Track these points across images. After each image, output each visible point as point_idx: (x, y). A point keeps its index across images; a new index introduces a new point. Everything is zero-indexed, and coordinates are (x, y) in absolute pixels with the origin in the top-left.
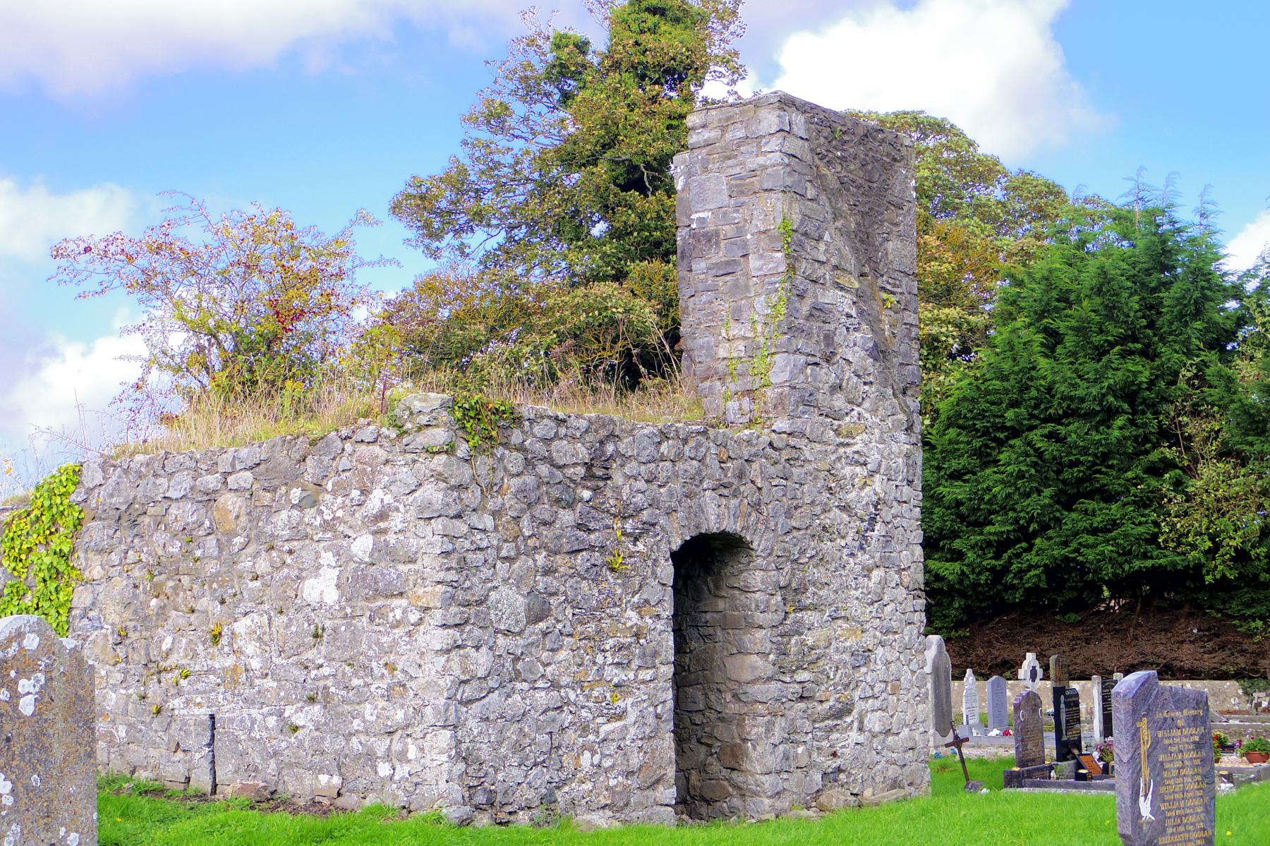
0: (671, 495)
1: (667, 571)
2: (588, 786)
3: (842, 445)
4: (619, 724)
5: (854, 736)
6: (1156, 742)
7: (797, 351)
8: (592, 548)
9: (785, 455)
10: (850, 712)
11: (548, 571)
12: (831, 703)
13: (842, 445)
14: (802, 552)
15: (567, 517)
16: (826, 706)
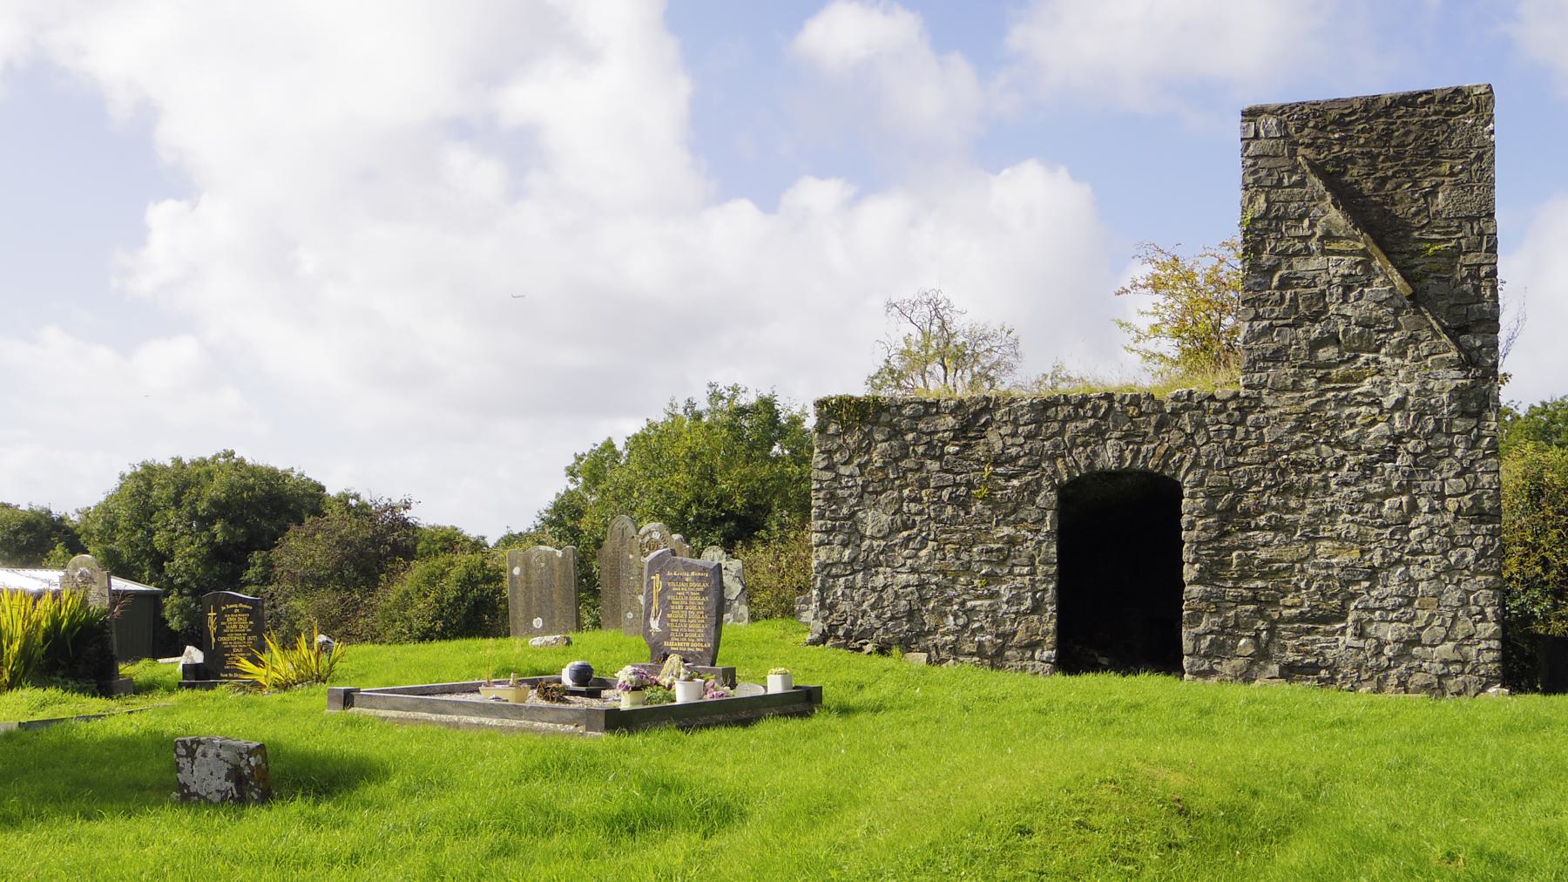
0: (1056, 446)
1: (1046, 498)
2: (952, 638)
3: (1333, 389)
4: (987, 602)
5: (1349, 638)
6: (665, 590)
7: (1257, 317)
8: (957, 485)
9: (1232, 405)
10: (1343, 619)
11: (918, 500)
12: (1305, 609)
13: (1333, 389)
14: (1251, 483)
15: (934, 466)
16: (1294, 611)
